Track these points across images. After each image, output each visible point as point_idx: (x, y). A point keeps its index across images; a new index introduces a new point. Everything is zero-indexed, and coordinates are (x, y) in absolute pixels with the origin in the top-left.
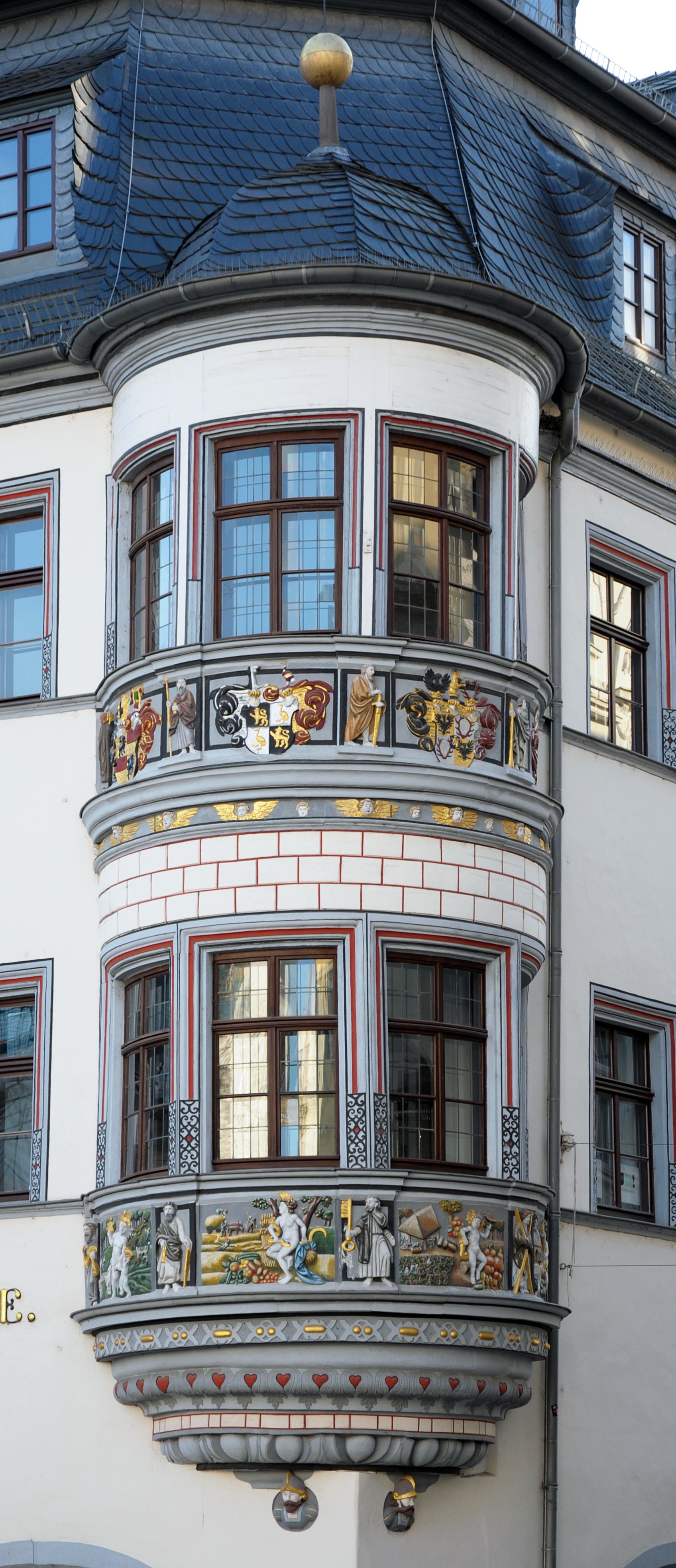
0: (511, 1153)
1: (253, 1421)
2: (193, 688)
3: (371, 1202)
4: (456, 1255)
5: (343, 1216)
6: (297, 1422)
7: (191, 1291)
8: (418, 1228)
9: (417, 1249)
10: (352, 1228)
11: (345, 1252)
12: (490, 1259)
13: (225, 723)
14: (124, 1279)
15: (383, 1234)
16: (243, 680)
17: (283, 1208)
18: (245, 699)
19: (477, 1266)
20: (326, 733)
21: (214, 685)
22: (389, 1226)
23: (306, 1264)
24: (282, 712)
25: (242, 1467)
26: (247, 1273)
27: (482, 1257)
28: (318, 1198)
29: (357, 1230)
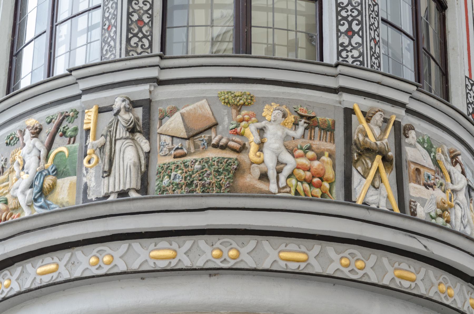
0: (350, 44)
3: (118, 104)
4: (242, 157)
5: (85, 127)
8: (182, 126)
9: (179, 151)
10: (95, 138)
11: (87, 169)
12: (304, 161)
15: (133, 139)
19: (279, 172)
22: (142, 129)
27: (287, 157)
28: (62, 114)
29: (101, 140)
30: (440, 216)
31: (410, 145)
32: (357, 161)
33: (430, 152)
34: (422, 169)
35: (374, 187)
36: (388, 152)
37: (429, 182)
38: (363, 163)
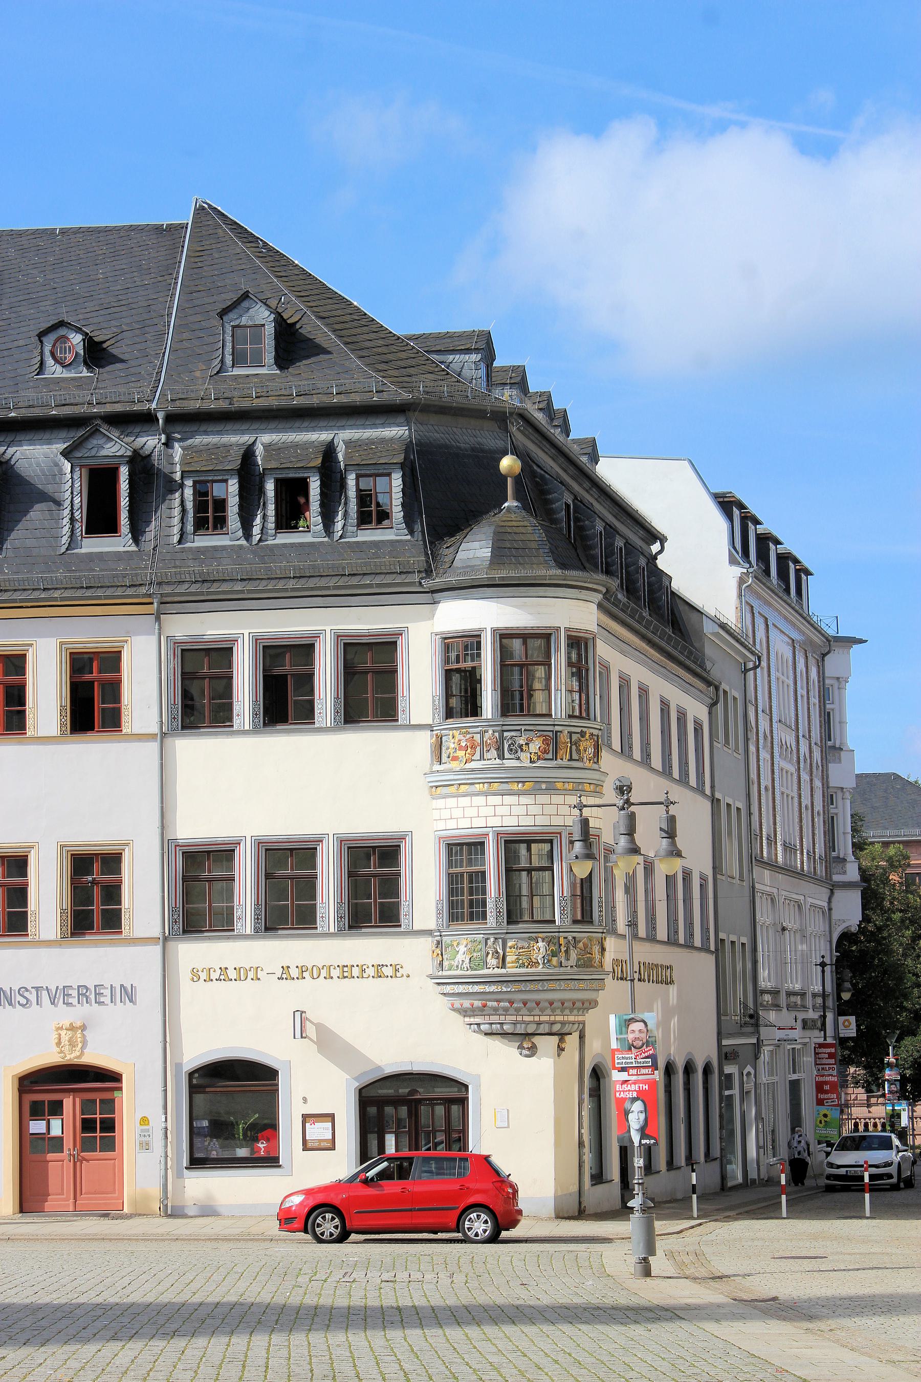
1: (519, 1018)
2: (497, 734)
3: (570, 938)
6: (537, 1019)
7: (503, 971)
13: (511, 750)
14: (466, 964)
16: (518, 734)
17: (540, 940)
18: (522, 741)
20: (550, 756)
21: (506, 734)
23: (549, 961)
24: (535, 746)
25: (504, 1034)
26: (526, 964)
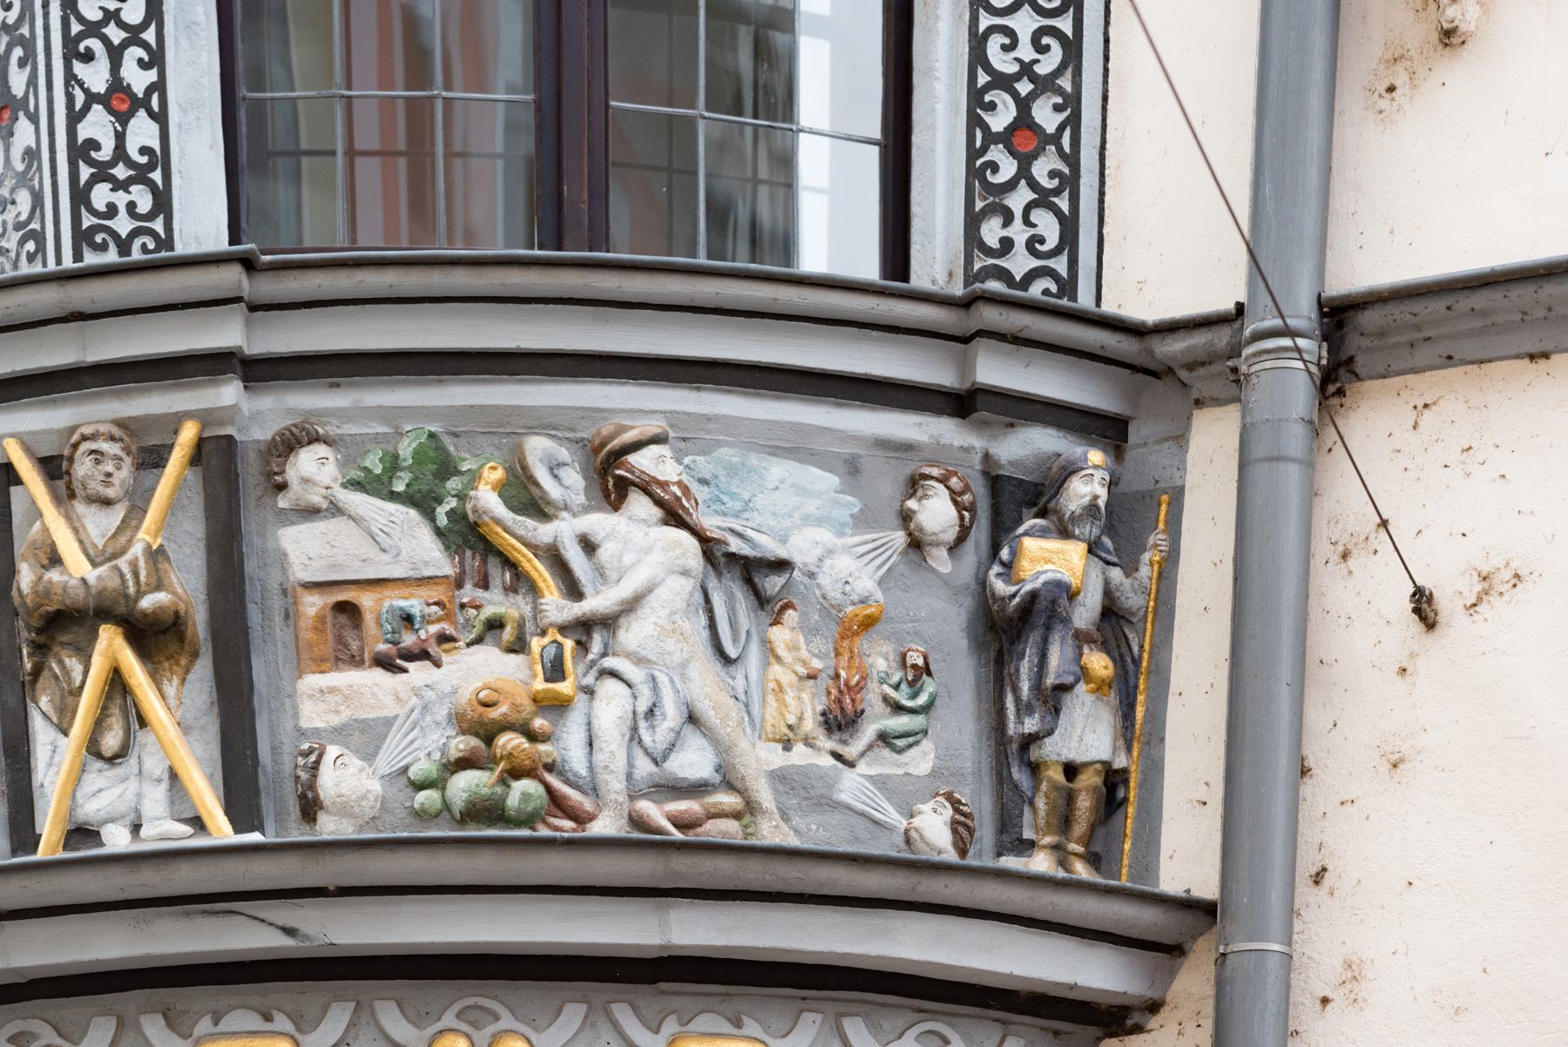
30: (465, 763)
31: (311, 513)
32: (37, 673)
33: (423, 502)
34: (366, 600)
35: (99, 755)
36: (137, 600)
37: (408, 640)
38: (56, 677)
